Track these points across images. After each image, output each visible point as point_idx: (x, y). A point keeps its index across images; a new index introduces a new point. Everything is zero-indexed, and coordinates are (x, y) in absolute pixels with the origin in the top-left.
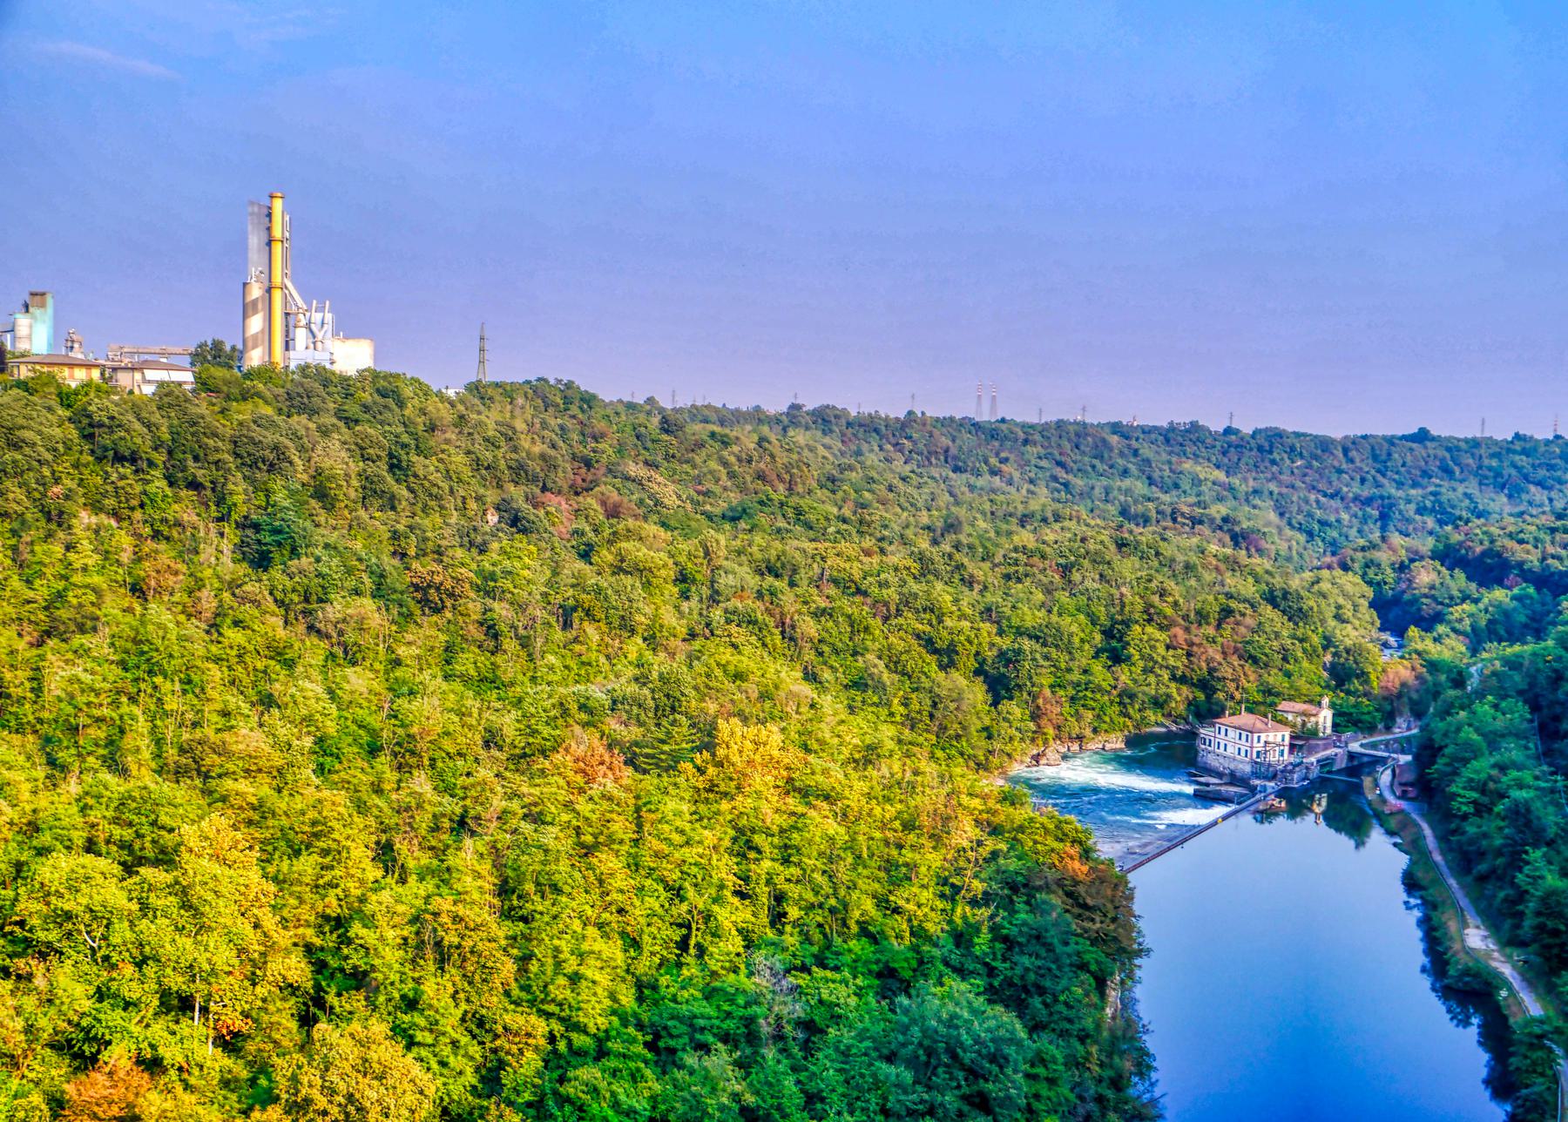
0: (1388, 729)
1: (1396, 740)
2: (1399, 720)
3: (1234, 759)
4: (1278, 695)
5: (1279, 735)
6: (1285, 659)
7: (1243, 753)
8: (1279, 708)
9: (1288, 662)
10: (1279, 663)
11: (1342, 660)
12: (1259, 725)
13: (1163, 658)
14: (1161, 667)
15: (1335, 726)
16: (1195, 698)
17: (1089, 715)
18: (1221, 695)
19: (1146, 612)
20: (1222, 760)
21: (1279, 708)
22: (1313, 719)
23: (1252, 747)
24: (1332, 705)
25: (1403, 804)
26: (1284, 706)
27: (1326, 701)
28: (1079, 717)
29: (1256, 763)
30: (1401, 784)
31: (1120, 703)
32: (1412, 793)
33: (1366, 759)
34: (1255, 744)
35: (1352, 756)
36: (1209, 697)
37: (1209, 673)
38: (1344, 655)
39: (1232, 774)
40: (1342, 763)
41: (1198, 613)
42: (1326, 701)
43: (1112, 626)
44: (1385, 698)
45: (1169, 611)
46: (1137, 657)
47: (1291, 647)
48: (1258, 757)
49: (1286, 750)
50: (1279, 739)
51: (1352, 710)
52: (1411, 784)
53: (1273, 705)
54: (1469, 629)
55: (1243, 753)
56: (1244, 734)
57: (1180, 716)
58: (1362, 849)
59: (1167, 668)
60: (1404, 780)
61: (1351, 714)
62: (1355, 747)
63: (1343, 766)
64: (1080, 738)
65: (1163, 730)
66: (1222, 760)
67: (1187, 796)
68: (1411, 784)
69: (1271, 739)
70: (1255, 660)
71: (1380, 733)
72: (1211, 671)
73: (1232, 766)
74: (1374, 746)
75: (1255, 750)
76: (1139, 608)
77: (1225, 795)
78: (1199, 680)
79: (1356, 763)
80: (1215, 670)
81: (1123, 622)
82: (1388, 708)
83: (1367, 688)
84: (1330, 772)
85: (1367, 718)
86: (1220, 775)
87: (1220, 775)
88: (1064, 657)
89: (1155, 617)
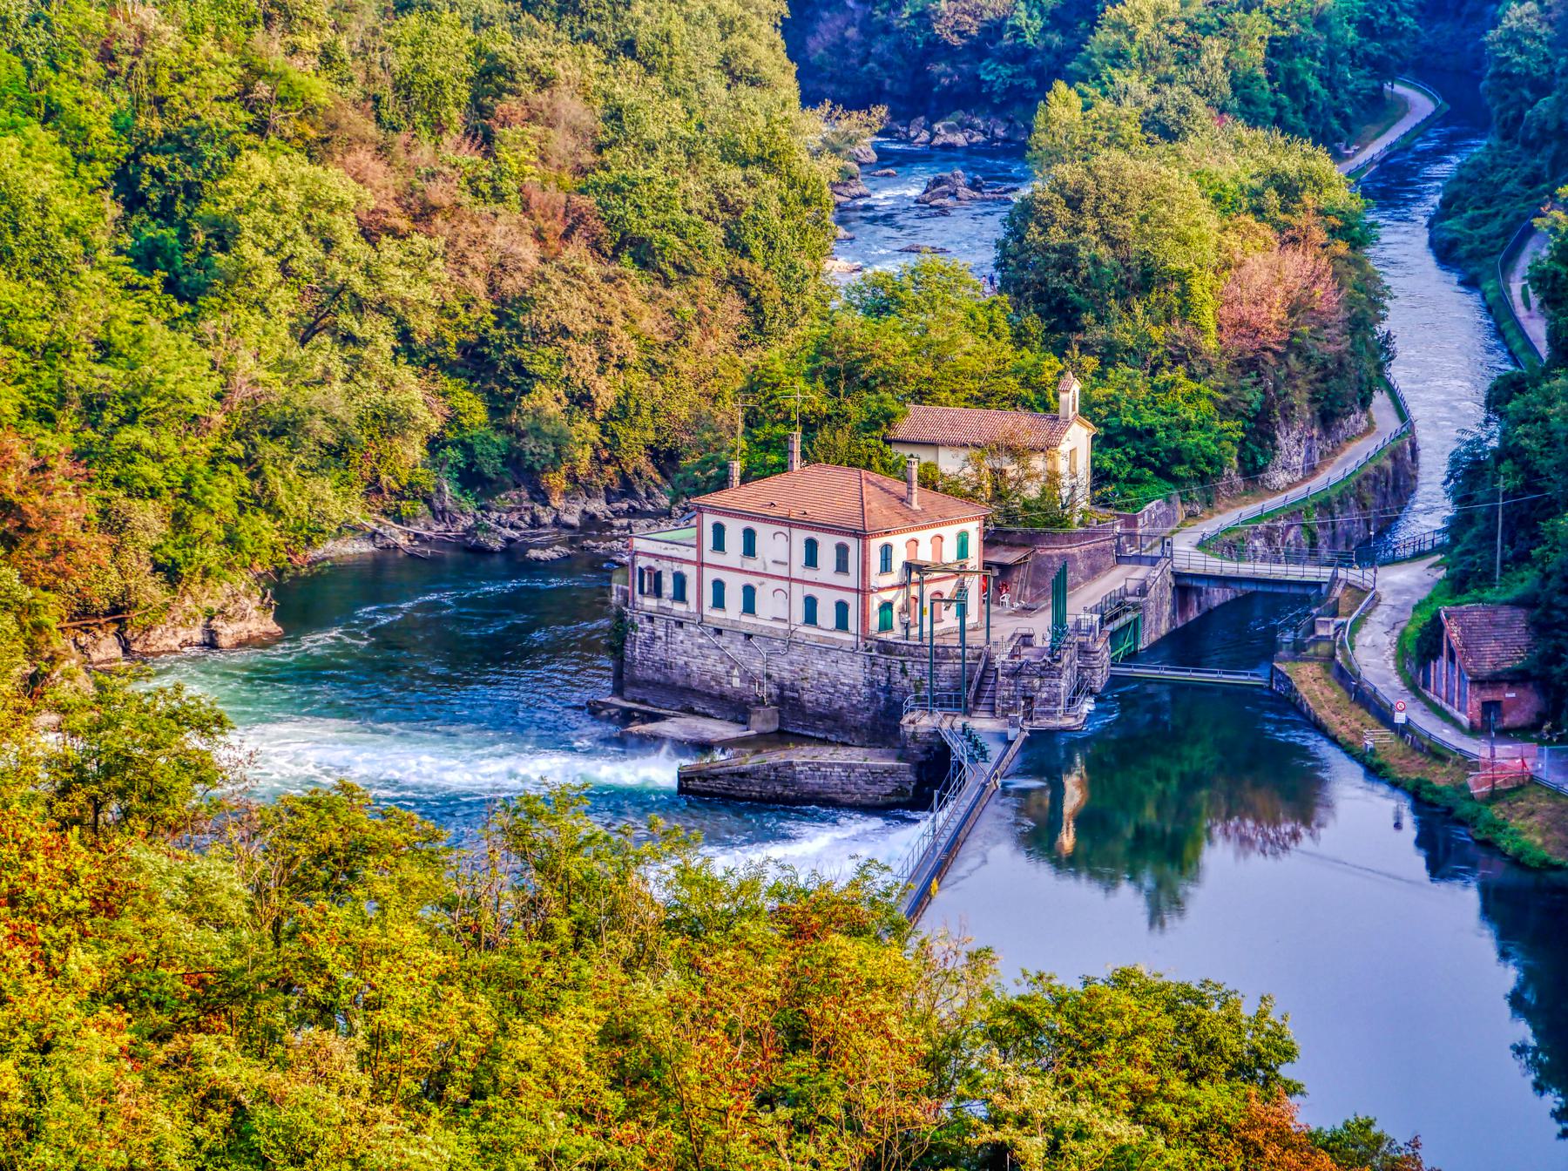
0: (1253, 473)
1: (1294, 512)
2: (1286, 440)
3: (790, 642)
4: (889, 379)
5: (950, 533)
6: (734, 243)
7: (827, 615)
8: (902, 430)
9: (745, 252)
10: (719, 259)
11: (1057, 236)
12: (878, 508)
13: (368, 272)
14: (359, 306)
15: (1100, 477)
16: (453, 420)
17: (149, 518)
18: (546, 401)
19: (244, 95)
20: (736, 649)
21: (902, 430)
22: (1038, 463)
23: (863, 592)
24: (1088, 408)
25: (1508, 755)
26: (913, 420)
27: (1071, 394)
28: (112, 523)
29: (886, 648)
30: (1480, 682)
31: (246, 461)
32: (1520, 704)
33: (1218, 596)
34: (876, 579)
35: (1185, 587)
36: (499, 408)
37: (502, 319)
38: (1062, 213)
39: (787, 701)
40: (1158, 623)
41: (403, 88)
42: (1071, 394)
43: (134, 157)
44: (1248, 365)
45: (320, 89)
46: (272, 275)
47: (747, 195)
48: (886, 626)
49: (974, 584)
50: (950, 554)
51: (1149, 419)
52: (1517, 678)
53: (880, 421)
54: (1221, 78)
55: (827, 615)
56: (827, 545)
57: (410, 490)
58: (1172, 922)
59: (382, 309)
60: (1486, 668)
61: (1151, 432)
62: (1187, 553)
63: (1164, 628)
64: (118, 612)
65: (366, 548)
66: (736, 649)
67: (614, 800)
68: (1517, 678)
69: (925, 555)
70: (643, 254)
71: (1235, 498)
72: (507, 310)
73: (783, 669)
74: (1231, 546)
75: (875, 602)
76: (223, 79)
77: (815, 783)
78: (463, 347)
79: (1193, 615)
80: (524, 302)
81: (173, 142)
82: (1254, 397)
83: (1177, 329)
84: (1132, 657)
85: (1198, 437)
86: (736, 708)
87: (736, 708)
88: (36, 295)
89: (275, 114)
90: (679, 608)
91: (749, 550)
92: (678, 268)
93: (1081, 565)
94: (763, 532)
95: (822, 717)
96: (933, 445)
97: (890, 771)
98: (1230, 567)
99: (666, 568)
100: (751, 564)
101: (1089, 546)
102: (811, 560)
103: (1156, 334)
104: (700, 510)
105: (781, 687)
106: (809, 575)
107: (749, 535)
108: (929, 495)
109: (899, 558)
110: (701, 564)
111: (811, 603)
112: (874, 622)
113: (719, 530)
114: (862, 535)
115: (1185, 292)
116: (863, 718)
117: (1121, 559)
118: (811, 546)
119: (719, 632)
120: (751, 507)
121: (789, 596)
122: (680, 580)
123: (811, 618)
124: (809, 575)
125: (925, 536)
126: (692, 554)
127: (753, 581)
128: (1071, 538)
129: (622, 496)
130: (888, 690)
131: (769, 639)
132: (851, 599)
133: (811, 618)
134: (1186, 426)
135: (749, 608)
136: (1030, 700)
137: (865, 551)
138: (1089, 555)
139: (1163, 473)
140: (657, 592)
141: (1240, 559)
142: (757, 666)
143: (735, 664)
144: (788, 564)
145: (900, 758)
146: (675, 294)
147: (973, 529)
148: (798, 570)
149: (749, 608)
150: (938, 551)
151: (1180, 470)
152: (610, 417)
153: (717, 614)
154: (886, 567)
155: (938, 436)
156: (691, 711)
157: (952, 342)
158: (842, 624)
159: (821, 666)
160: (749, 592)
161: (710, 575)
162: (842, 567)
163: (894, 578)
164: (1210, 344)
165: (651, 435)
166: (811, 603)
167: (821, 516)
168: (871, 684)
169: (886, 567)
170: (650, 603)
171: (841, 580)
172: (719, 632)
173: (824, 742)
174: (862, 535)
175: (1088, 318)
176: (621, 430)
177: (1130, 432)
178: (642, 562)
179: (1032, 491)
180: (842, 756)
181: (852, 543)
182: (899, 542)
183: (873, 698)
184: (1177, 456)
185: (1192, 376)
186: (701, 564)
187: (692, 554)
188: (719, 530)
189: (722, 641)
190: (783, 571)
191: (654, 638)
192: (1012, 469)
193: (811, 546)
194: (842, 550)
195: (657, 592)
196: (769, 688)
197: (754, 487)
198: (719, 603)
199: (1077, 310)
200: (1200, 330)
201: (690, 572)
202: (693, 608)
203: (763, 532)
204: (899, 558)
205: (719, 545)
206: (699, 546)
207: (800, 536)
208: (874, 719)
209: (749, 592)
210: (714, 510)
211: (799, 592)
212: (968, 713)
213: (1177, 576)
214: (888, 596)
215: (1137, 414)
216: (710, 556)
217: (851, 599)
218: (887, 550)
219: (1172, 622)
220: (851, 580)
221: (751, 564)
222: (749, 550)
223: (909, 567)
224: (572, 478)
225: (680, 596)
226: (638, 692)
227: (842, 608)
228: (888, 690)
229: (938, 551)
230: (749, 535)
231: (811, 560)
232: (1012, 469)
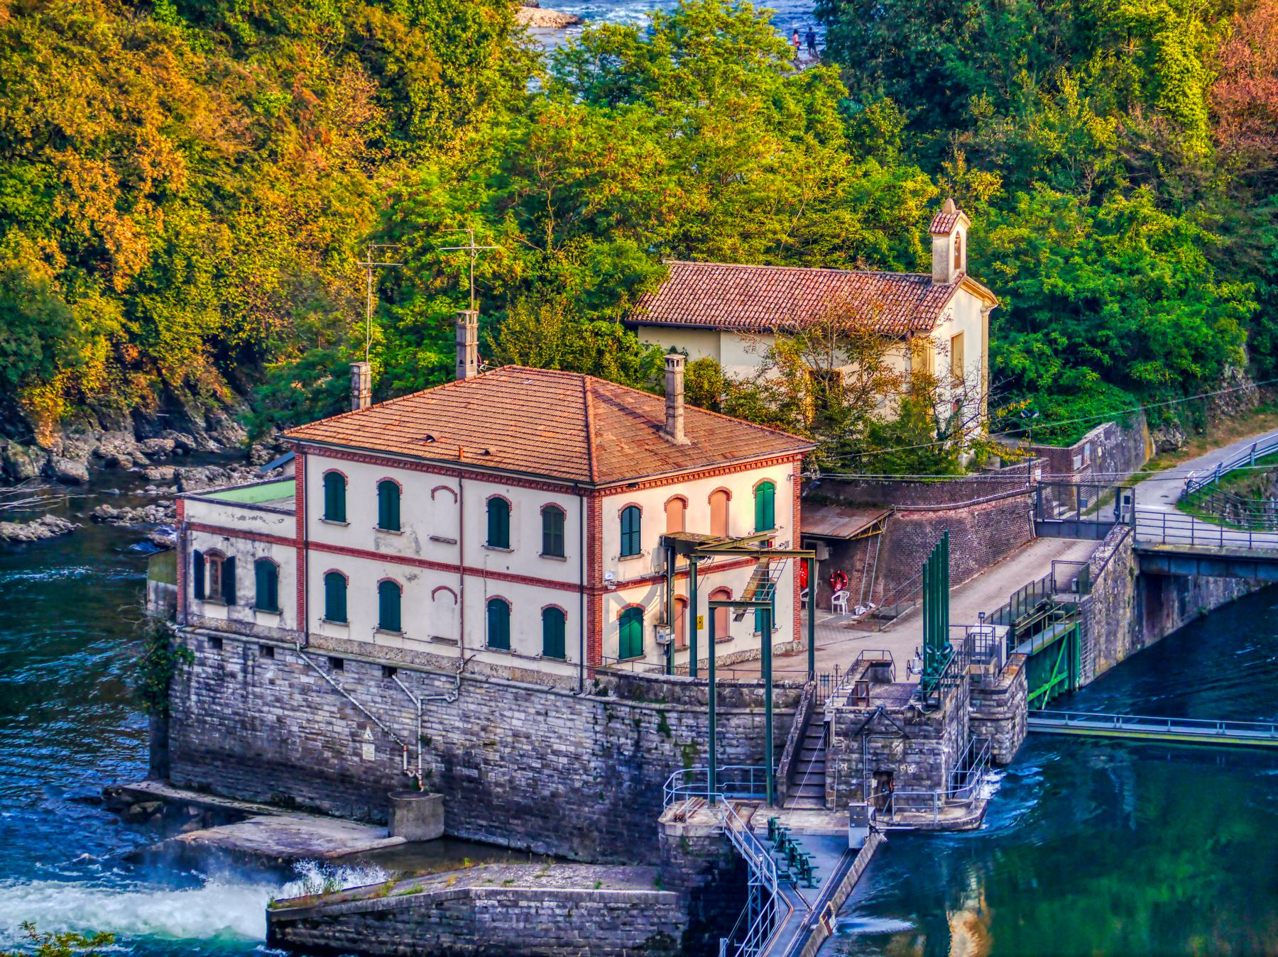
5: (742, 485)
8: (656, 305)
21: (656, 305)
22: (896, 360)
23: (591, 590)
29: (633, 688)
34: (614, 568)
48: (631, 649)
49: (785, 574)
51: (1092, 280)
61: (1094, 303)
63: (1121, 648)
66: (368, 693)
69: (699, 524)
75: (612, 608)
79: (1172, 624)
83: (1138, 122)
85: (1174, 314)
90: (266, 622)
91: (389, 519)
92: (258, 23)
93: (973, 538)
94: (414, 487)
95: (521, 812)
96: (711, 330)
97: (642, 906)
98: (1236, 540)
99: (238, 549)
100: (392, 544)
101: (986, 506)
102: (499, 536)
103: (1103, 130)
104: (302, 449)
105: (448, 758)
106: (496, 561)
107: (389, 494)
108: (704, 418)
109: (651, 535)
110: (303, 545)
111: (499, 612)
112: (611, 642)
113: (335, 484)
114: (588, 490)
115: (1152, 57)
116: (593, 811)
117: (1044, 529)
118: (499, 512)
119: (337, 663)
120: (393, 442)
121: (459, 598)
122: (267, 573)
123: (499, 637)
124: (496, 561)
125: (698, 492)
126: (288, 527)
127: (397, 572)
128: (956, 492)
129: (164, 425)
130: (637, 762)
131: (425, 676)
132: (569, 602)
133: (499, 637)
134: (1156, 292)
135: (390, 620)
136: (886, 778)
137: (593, 517)
138: (987, 520)
139: (1116, 375)
140: (228, 595)
141: (1255, 525)
142: (405, 723)
143: (367, 720)
144: (460, 543)
145: (658, 883)
146: (251, 68)
147: (782, 476)
148: (476, 554)
149: (390, 620)
150: (721, 516)
151: (1145, 370)
152: (140, 286)
153: (334, 632)
154: (630, 547)
155: (719, 314)
156: (290, 805)
157: (742, 149)
158: (554, 647)
159: (517, 721)
160: (390, 594)
161: (320, 564)
162: (553, 546)
163: (644, 565)
164: (1198, 147)
165: (213, 319)
166: (499, 612)
167: (514, 456)
168: (606, 752)
169: (630, 547)
170: (215, 614)
171: (551, 570)
172: (337, 663)
173: (525, 855)
174: (588, 490)
175: (981, 104)
176: (160, 309)
177: (1058, 303)
178: (201, 542)
179: (886, 410)
180: (557, 879)
181: (570, 504)
182: (652, 501)
183: (610, 776)
184: (1141, 345)
185: (1165, 204)
186: (303, 545)
187: (288, 527)
188: (335, 484)
189: (344, 679)
190: (447, 555)
191: (222, 675)
192: (849, 372)
193: (499, 512)
194: (552, 517)
195: (228, 595)
196: (424, 764)
197: (396, 407)
198: (337, 612)
199: (961, 90)
200: (1180, 122)
201: (285, 557)
202: (291, 621)
203: (414, 487)
204: (651, 535)
205: (336, 511)
206: (301, 513)
207: (478, 494)
208: (612, 813)
209: (390, 594)
210: (326, 450)
211: (478, 593)
212: (777, 801)
213: (1144, 555)
214: (634, 596)
215: (1069, 272)
216: (319, 531)
217: (569, 602)
218: (631, 517)
219: (1136, 638)
220: (569, 570)
221: (392, 544)
222: (389, 519)
223: (671, 545)
224: (75, 395)
225: (267, 601)
226: (198, 774)
227: (553, 619)
228: (637, 762)
229: (721, 516)
230: (389, 494)
231: (499, 536)
232: (849, 372)
